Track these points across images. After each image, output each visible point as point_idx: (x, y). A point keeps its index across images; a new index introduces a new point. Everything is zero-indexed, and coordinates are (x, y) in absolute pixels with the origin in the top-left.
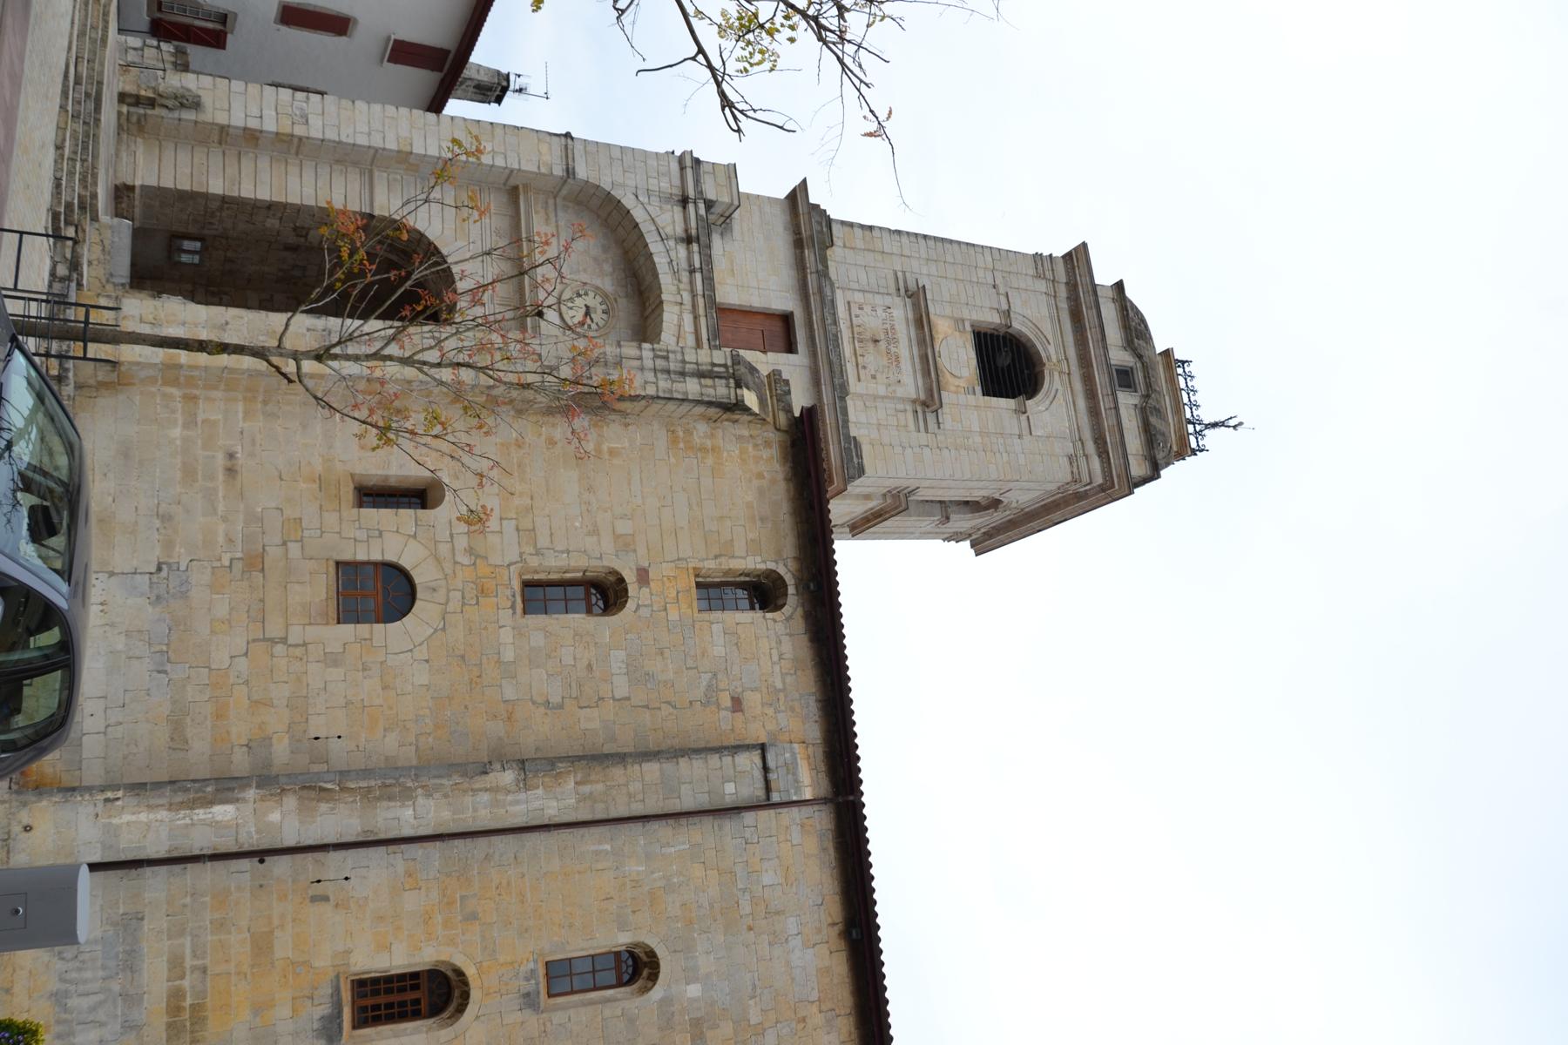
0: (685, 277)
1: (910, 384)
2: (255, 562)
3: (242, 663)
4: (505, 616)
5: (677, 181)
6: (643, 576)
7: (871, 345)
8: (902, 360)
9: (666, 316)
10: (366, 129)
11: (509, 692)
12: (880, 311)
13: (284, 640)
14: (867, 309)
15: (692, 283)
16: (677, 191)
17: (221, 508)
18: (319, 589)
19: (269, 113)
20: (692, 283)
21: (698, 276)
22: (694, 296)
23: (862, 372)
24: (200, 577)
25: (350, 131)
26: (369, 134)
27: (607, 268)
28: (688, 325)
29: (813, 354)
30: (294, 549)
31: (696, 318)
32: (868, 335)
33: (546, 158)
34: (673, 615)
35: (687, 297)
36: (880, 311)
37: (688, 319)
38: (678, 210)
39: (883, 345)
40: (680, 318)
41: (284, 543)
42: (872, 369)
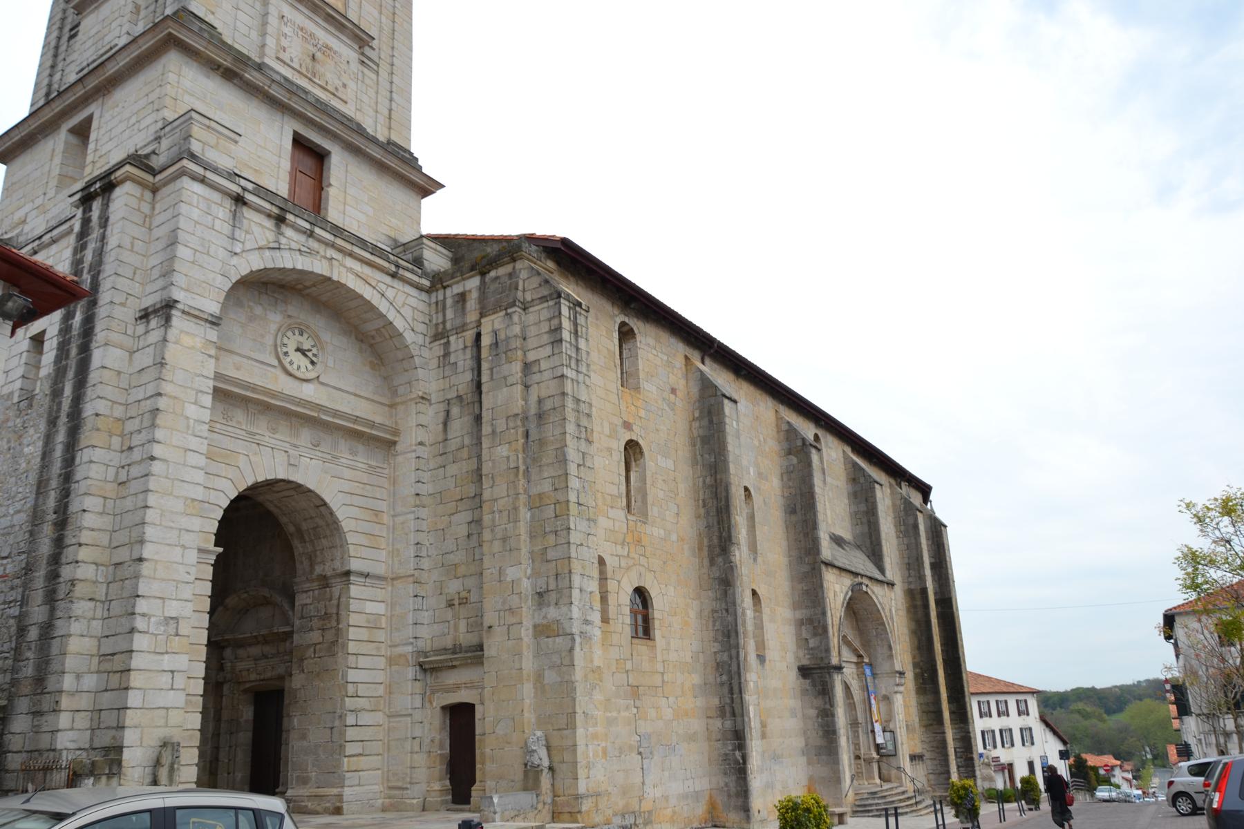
0: (313, 244)
1: (345, 51)
2: (635, 692)
3: (671, 699)
4: (648, 529)
5: (216, 196)
6: (627, 426)
7: (318, 66)
8: (330, 44)
9: (351, 285)
10: (178, 550)
11: (674, 537)
12: (287, 30)
13: (663, 674)
14: (284, 43)
15: (320, 240)
16: (228, 203)
17: (615, 714)
18: (642, 647)
19: (167, 662)
20: (320, 240)
21: (317, 231)
22: (333, 246)
23: (339, 94)
24: (644, 728)
25: (181, 569)
26: (184, 547)
27: (258, 310)
28: (357, 266)
29: (335, 137)
30: (629, 666)
31: (351, 255)
32: (308, 60)
33: (198, 342)
34: (642, 413)
35: (331, 253)
36: (287, 30)
37: (349, 262)
38: (247, 212)
39: (319, 55)
40: (350, 270)
41: (627, 672)
42: (338, 83)
